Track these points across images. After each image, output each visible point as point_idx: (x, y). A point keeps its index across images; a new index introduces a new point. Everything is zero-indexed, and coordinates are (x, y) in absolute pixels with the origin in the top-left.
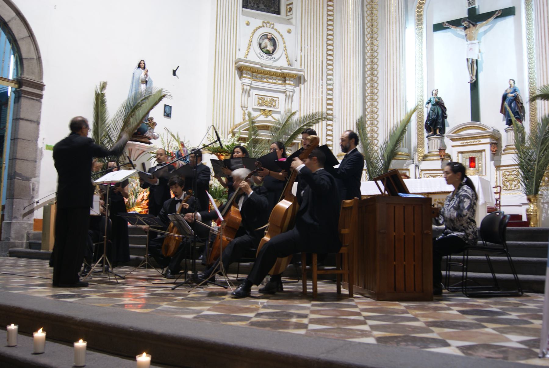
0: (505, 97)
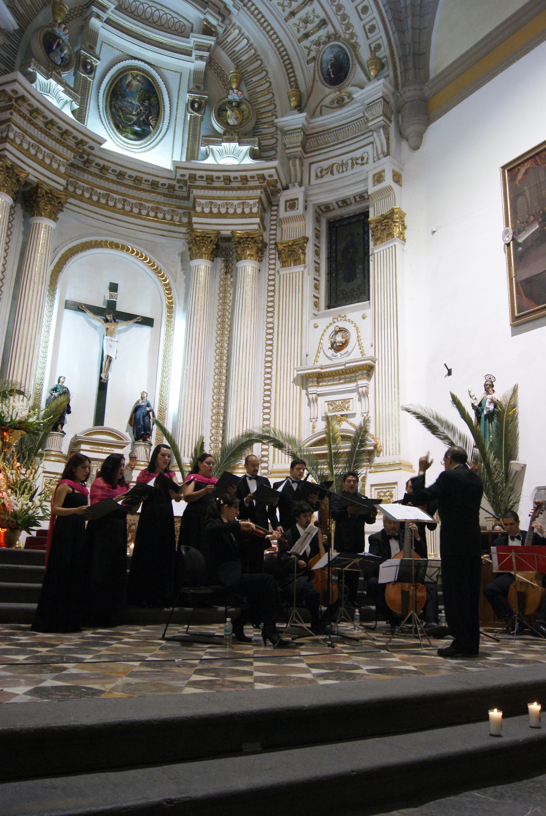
0: (137, 409)
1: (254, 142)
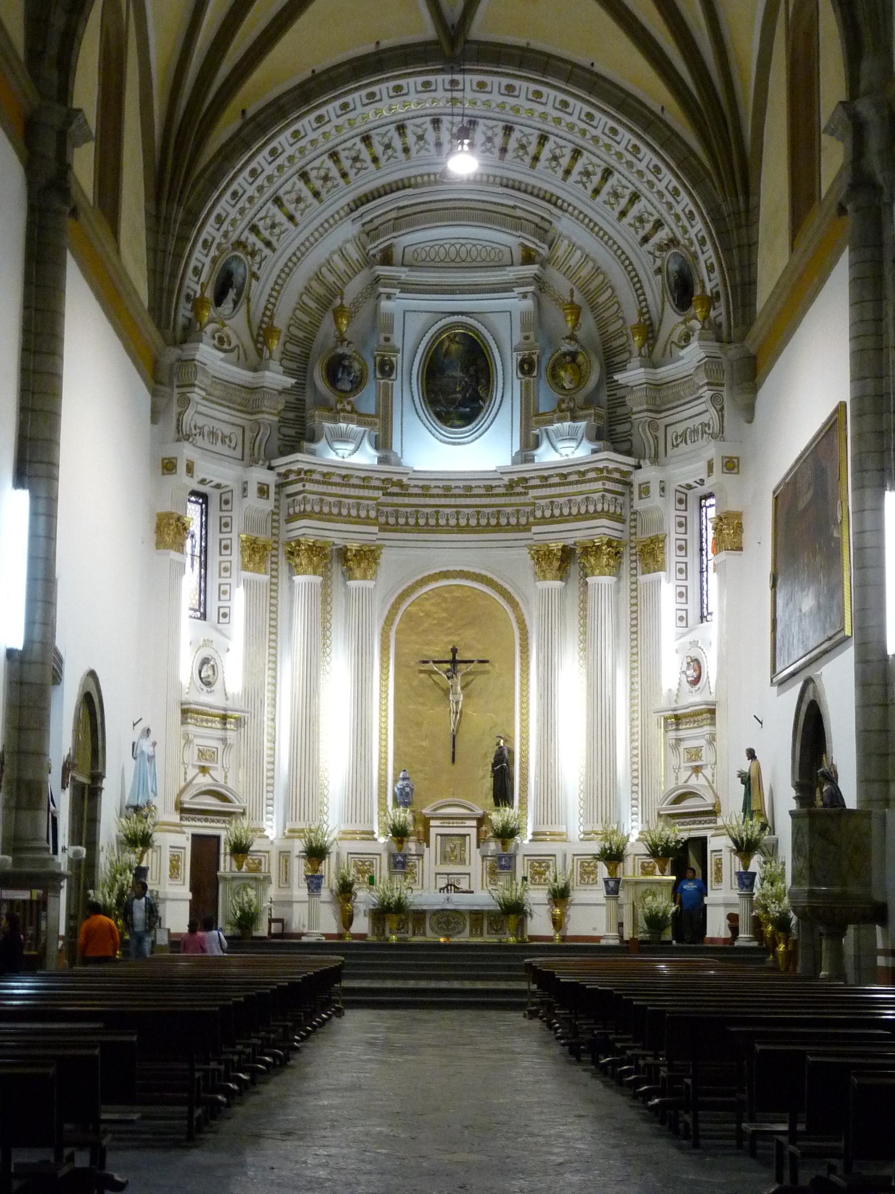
1: (590, 415)
